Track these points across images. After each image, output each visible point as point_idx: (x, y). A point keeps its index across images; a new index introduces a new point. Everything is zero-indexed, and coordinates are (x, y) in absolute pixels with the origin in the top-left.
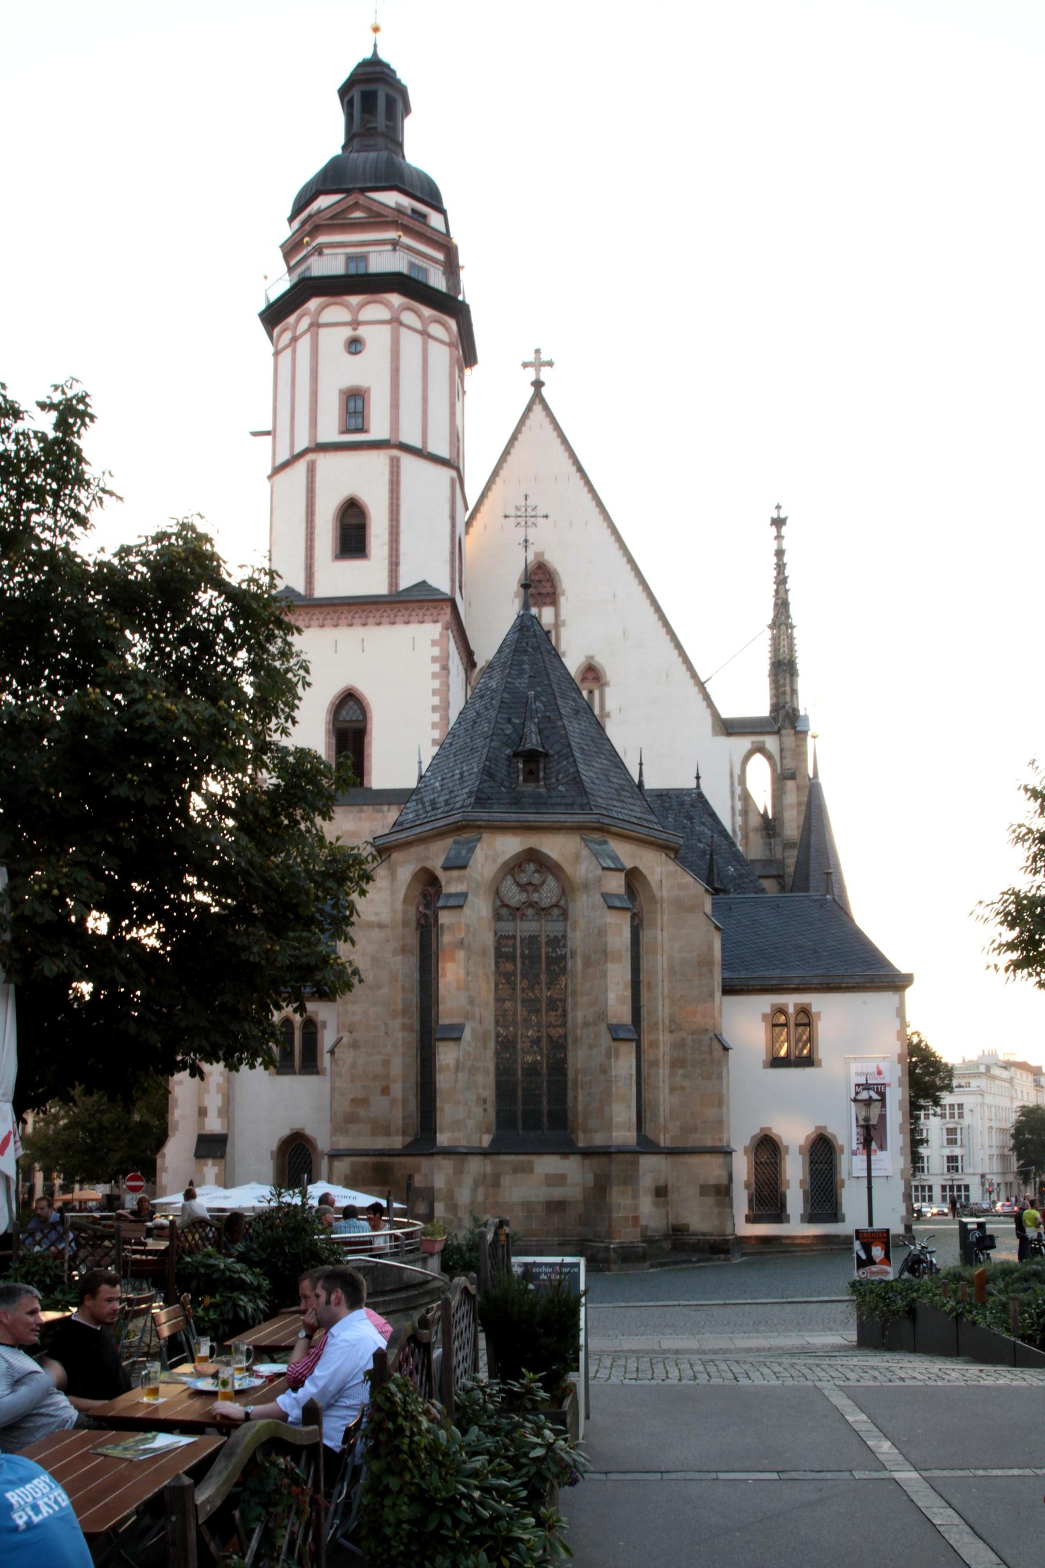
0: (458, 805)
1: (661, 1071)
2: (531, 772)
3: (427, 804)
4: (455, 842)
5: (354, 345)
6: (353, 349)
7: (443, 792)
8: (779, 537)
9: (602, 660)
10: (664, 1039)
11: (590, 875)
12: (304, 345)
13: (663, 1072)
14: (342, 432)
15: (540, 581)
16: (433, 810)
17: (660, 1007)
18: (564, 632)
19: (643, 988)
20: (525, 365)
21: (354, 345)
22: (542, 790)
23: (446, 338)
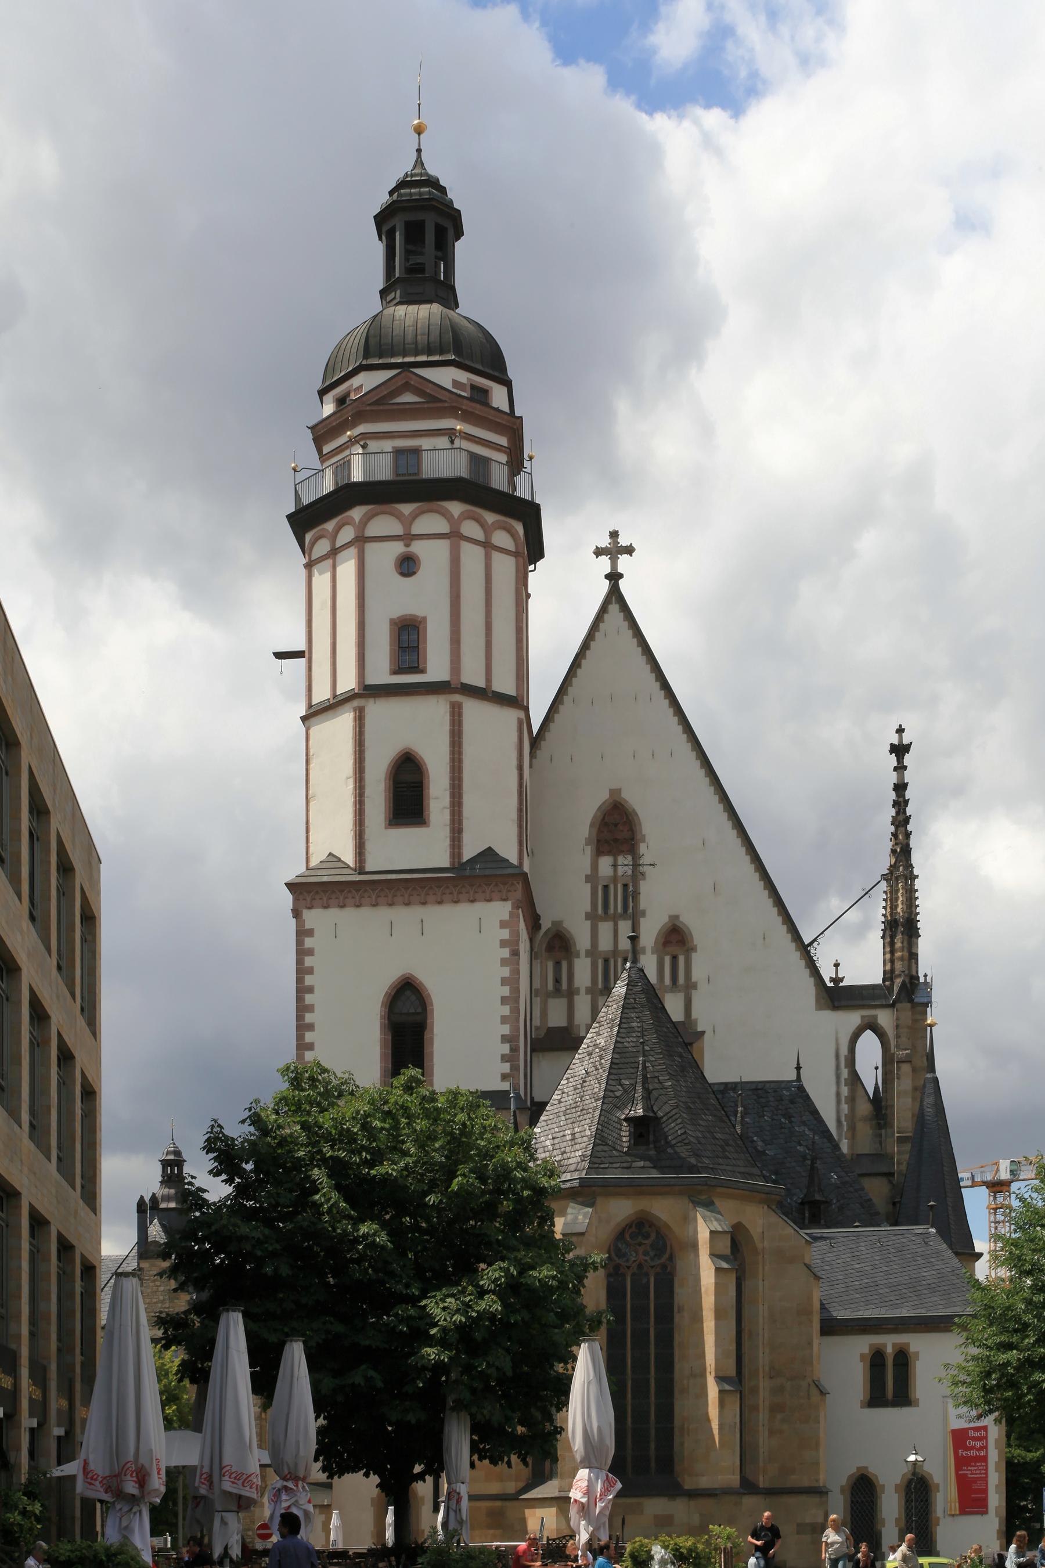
0: (572, 1168)
1: (761, 1415)
2: (641, 1135)
5: (407, 566)
7: (555, 1153)
8: (900, 768)
9: (690, 921)
10: (764, 1385)
13: (763, 1416)
14: (395, 672)
15: (616, 825)
17: (761, 1355)
19: (745, 1336)
20: (599, 552)
21: (407, 566)
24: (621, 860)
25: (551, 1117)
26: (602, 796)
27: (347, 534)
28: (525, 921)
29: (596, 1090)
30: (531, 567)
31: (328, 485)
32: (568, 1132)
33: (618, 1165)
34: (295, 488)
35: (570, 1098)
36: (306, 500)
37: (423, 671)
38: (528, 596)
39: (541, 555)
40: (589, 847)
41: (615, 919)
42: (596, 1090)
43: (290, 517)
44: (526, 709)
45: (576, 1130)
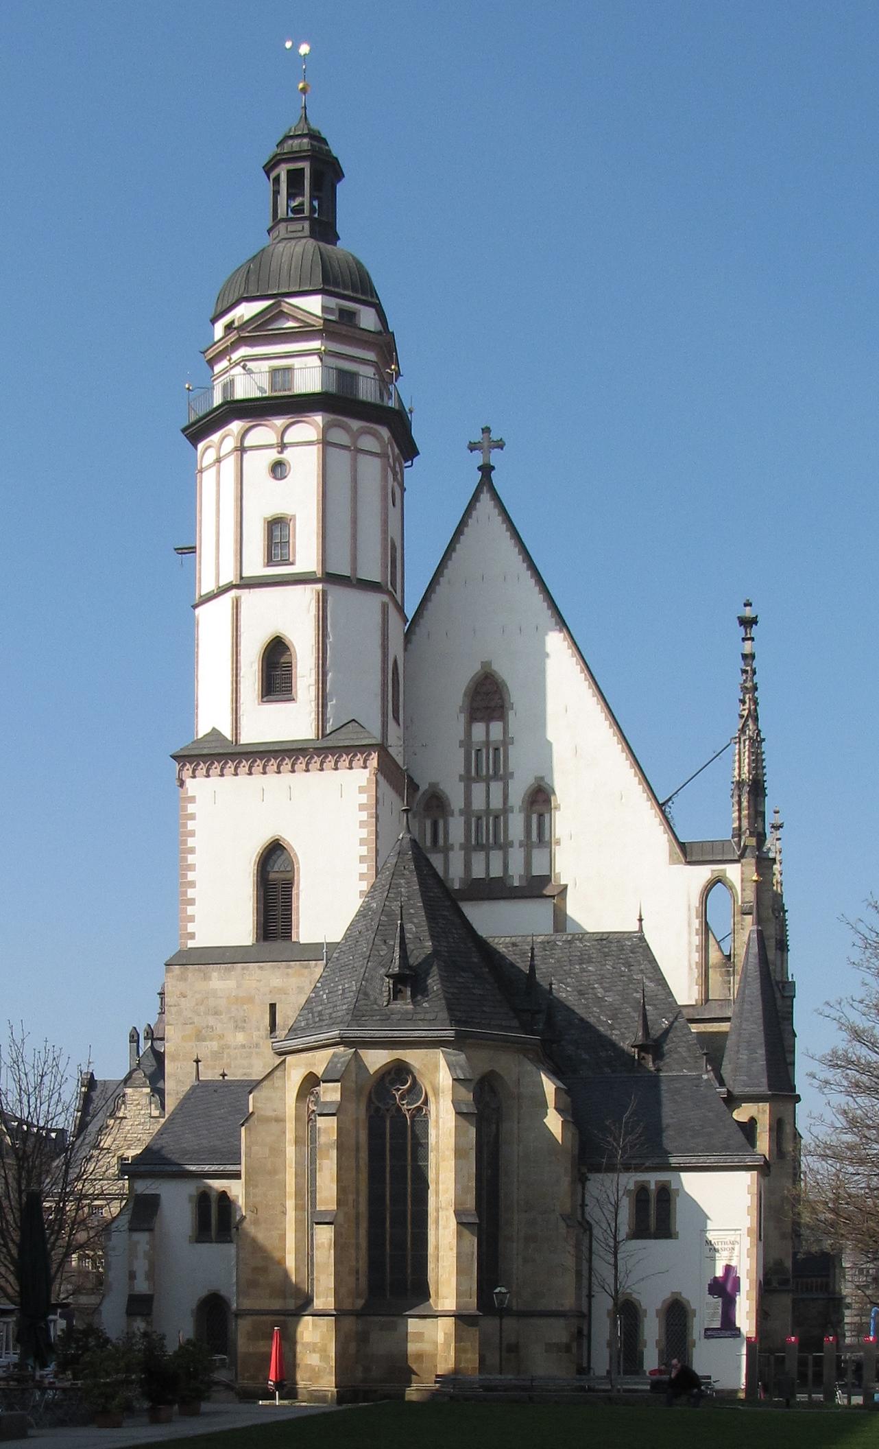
0: (339, 1020)
3: (316, 1014)
5: (278, 469)
18: (512, 750)
21: (278, 469)
26: (474, 669)
27: (230, 444)
29: (365, 949)
31: (217, 400)
32: (340, 987)
33: (378, 1017)
37: (292, 564)
38: (403, 490)
39: (416, 453)
40: (463, 715)
41: (488, 780)
42: (365, 949)
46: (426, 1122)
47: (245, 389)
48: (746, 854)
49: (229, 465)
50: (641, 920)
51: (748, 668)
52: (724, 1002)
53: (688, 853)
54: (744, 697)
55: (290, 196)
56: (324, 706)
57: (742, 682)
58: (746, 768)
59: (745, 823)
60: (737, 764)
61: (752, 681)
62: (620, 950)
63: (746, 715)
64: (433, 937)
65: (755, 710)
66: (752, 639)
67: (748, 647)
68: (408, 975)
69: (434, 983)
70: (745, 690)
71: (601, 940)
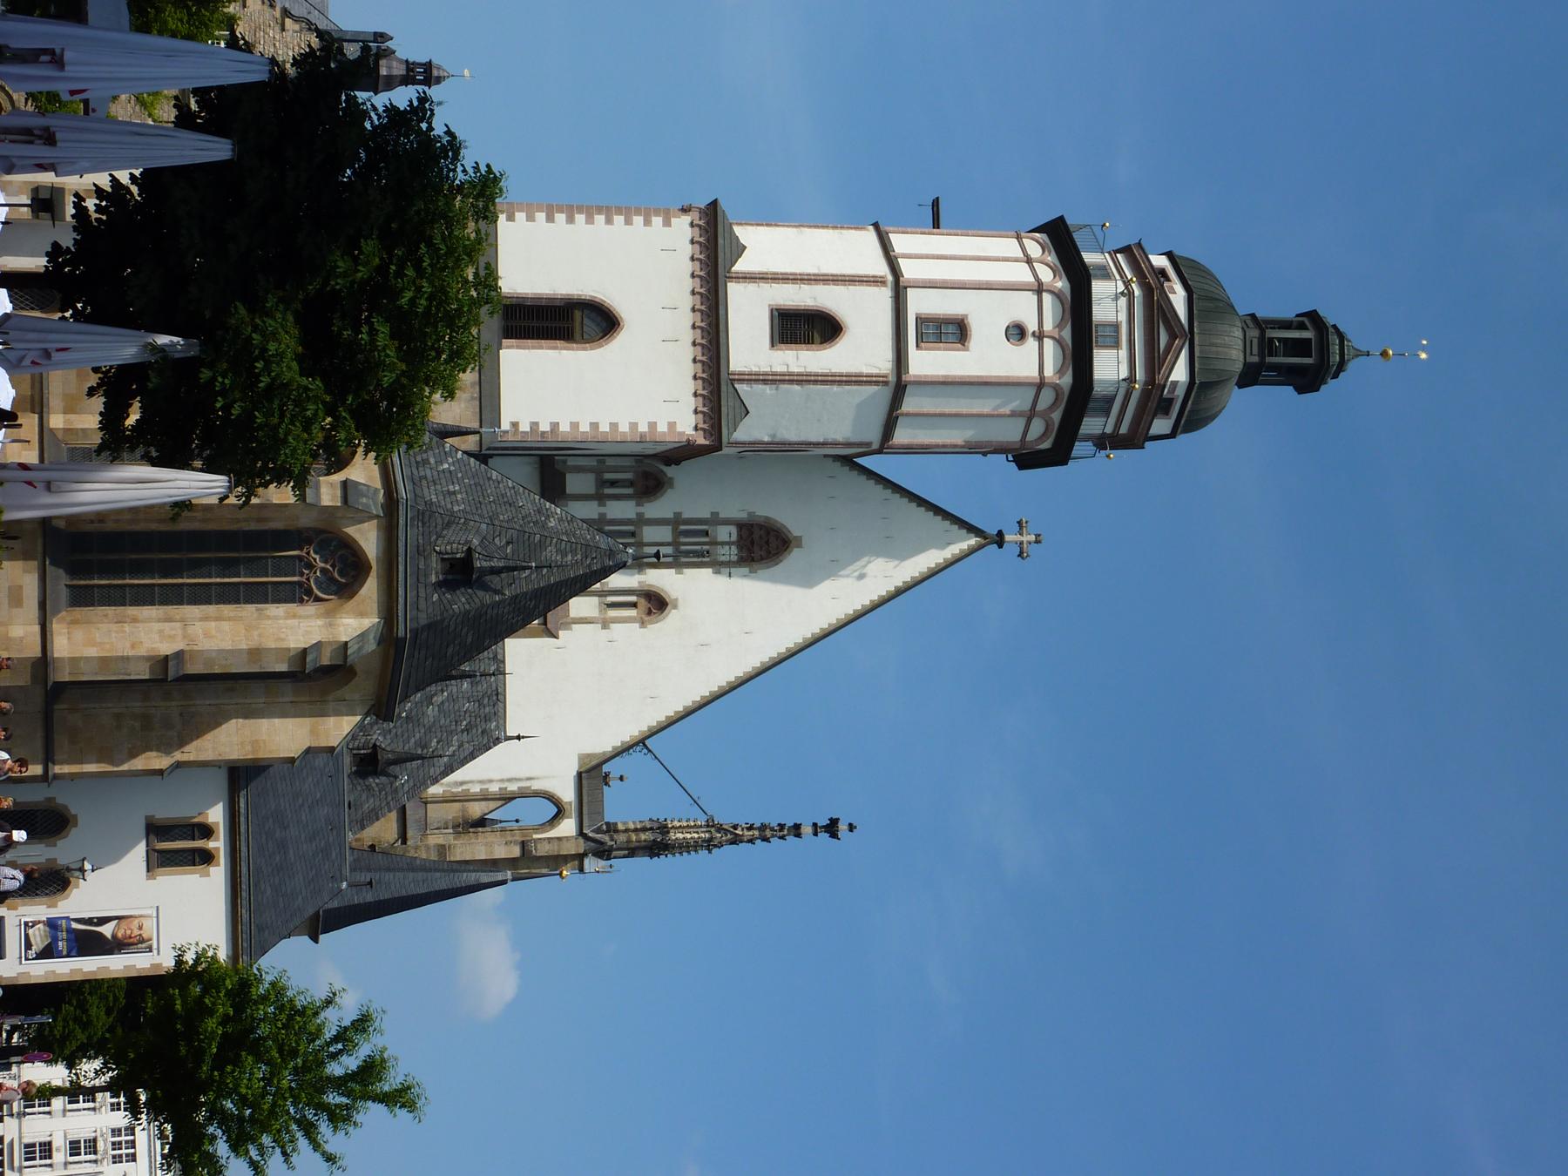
0: (418, 491)
1: (138, 704)
3: (424, 456)
4: (376, 490)
6: (1011, 331)
7: (435, 473)
11: (341, 628)
12: (1022, 274)
16: (417, 463)
22: (433, 579)
23: (1032, 436)
24: (734, 550)
25: (473, 470)
28: (675, 448)
29: (501, 517)
30: (1010, 458)
31: (1090, 258)
33: (421, 541)
34: (1085, 226)
35: (494, 489)
36: (1075, 236)
37: (917, 346)
38: (985, 454)
39: (1021, 467)
43: (1061, 219)
44: (879, 451)
45: (459, 496)
46: (292, 601)
47: (1101, 290)
48: (589, 843)
49: (1022, 274)
50: (519, 738)
51: (785, 832)
52: (423, 823)
53: (592, 775)
54: (755, 829)
55: (1284, 341)
56: (765, 382)
57: (771, 825)
58: (680, 836)
59: (622, 838)
60: (685, 824)
61: (773, 836)
62: (485, 717)
63: (737, 832)
64: (514, 598)
65: (742, 842)
66: (816, 834)
67: (807, 830)
68: (472, 576)
69: (461, 602)
70: (763, 827)
71: (497, 695)
